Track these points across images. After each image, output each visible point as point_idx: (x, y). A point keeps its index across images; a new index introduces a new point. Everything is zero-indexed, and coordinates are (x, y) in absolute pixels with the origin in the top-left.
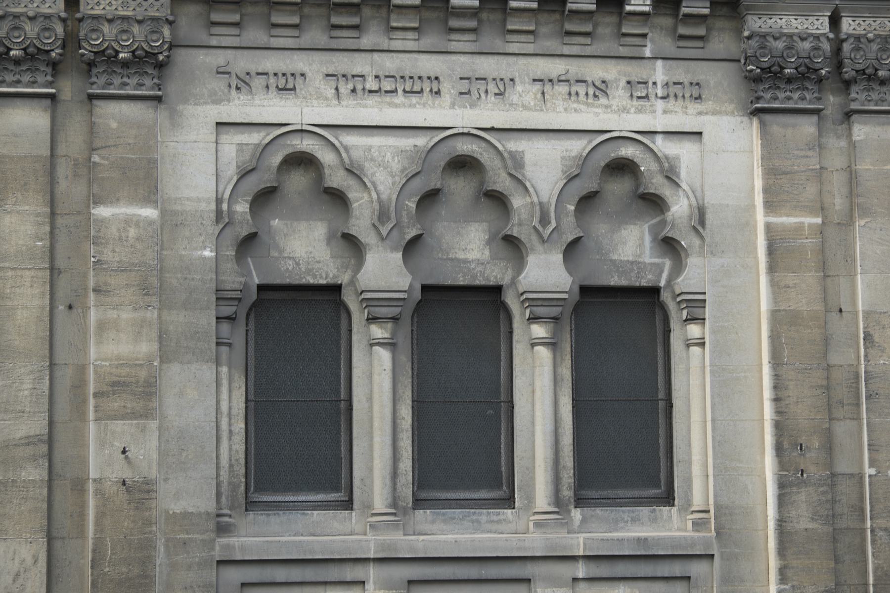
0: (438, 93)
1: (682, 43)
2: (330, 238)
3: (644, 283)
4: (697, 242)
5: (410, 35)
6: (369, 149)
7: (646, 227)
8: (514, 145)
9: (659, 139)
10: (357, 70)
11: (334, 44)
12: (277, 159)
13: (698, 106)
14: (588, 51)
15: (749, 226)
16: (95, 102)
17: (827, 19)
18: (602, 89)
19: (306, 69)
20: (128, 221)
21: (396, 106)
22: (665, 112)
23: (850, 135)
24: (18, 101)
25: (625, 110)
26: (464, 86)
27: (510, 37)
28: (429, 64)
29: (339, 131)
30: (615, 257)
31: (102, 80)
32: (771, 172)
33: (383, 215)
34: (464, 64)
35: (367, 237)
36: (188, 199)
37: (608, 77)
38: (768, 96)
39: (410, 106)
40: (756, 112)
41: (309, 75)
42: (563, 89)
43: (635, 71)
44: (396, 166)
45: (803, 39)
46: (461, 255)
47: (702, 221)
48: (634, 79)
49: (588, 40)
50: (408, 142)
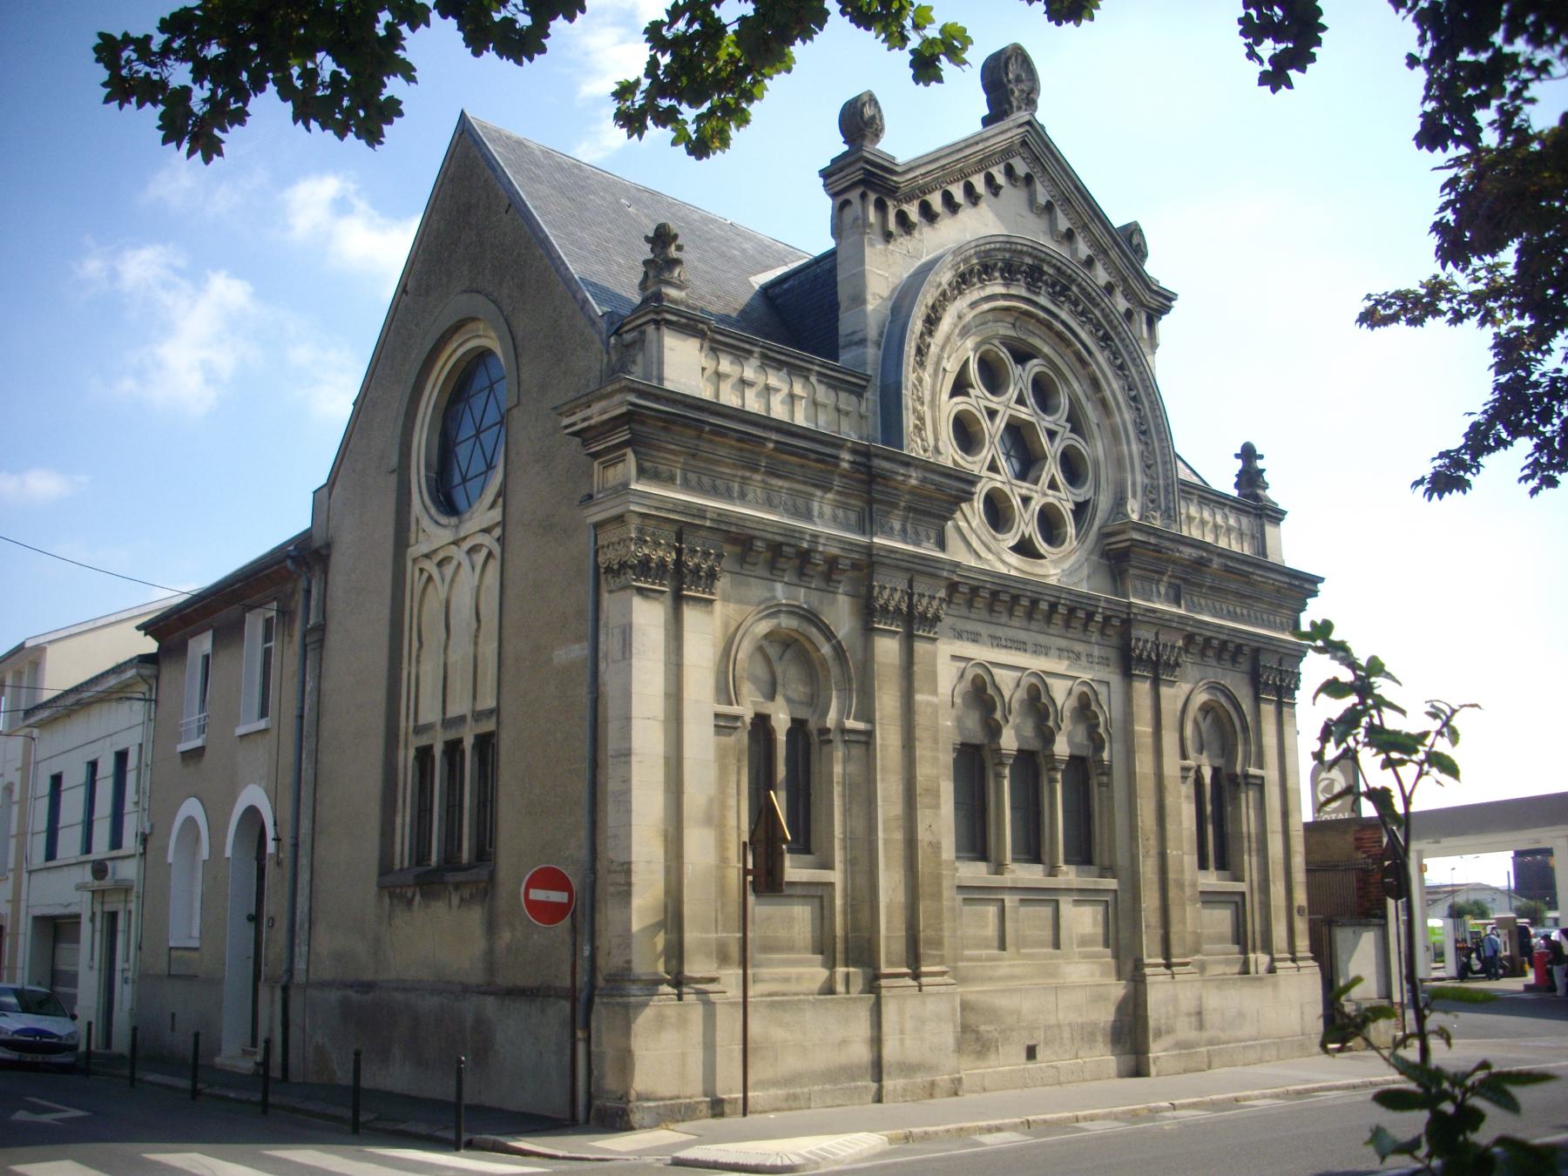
13: (1107, 669)
28: (1022, 635)
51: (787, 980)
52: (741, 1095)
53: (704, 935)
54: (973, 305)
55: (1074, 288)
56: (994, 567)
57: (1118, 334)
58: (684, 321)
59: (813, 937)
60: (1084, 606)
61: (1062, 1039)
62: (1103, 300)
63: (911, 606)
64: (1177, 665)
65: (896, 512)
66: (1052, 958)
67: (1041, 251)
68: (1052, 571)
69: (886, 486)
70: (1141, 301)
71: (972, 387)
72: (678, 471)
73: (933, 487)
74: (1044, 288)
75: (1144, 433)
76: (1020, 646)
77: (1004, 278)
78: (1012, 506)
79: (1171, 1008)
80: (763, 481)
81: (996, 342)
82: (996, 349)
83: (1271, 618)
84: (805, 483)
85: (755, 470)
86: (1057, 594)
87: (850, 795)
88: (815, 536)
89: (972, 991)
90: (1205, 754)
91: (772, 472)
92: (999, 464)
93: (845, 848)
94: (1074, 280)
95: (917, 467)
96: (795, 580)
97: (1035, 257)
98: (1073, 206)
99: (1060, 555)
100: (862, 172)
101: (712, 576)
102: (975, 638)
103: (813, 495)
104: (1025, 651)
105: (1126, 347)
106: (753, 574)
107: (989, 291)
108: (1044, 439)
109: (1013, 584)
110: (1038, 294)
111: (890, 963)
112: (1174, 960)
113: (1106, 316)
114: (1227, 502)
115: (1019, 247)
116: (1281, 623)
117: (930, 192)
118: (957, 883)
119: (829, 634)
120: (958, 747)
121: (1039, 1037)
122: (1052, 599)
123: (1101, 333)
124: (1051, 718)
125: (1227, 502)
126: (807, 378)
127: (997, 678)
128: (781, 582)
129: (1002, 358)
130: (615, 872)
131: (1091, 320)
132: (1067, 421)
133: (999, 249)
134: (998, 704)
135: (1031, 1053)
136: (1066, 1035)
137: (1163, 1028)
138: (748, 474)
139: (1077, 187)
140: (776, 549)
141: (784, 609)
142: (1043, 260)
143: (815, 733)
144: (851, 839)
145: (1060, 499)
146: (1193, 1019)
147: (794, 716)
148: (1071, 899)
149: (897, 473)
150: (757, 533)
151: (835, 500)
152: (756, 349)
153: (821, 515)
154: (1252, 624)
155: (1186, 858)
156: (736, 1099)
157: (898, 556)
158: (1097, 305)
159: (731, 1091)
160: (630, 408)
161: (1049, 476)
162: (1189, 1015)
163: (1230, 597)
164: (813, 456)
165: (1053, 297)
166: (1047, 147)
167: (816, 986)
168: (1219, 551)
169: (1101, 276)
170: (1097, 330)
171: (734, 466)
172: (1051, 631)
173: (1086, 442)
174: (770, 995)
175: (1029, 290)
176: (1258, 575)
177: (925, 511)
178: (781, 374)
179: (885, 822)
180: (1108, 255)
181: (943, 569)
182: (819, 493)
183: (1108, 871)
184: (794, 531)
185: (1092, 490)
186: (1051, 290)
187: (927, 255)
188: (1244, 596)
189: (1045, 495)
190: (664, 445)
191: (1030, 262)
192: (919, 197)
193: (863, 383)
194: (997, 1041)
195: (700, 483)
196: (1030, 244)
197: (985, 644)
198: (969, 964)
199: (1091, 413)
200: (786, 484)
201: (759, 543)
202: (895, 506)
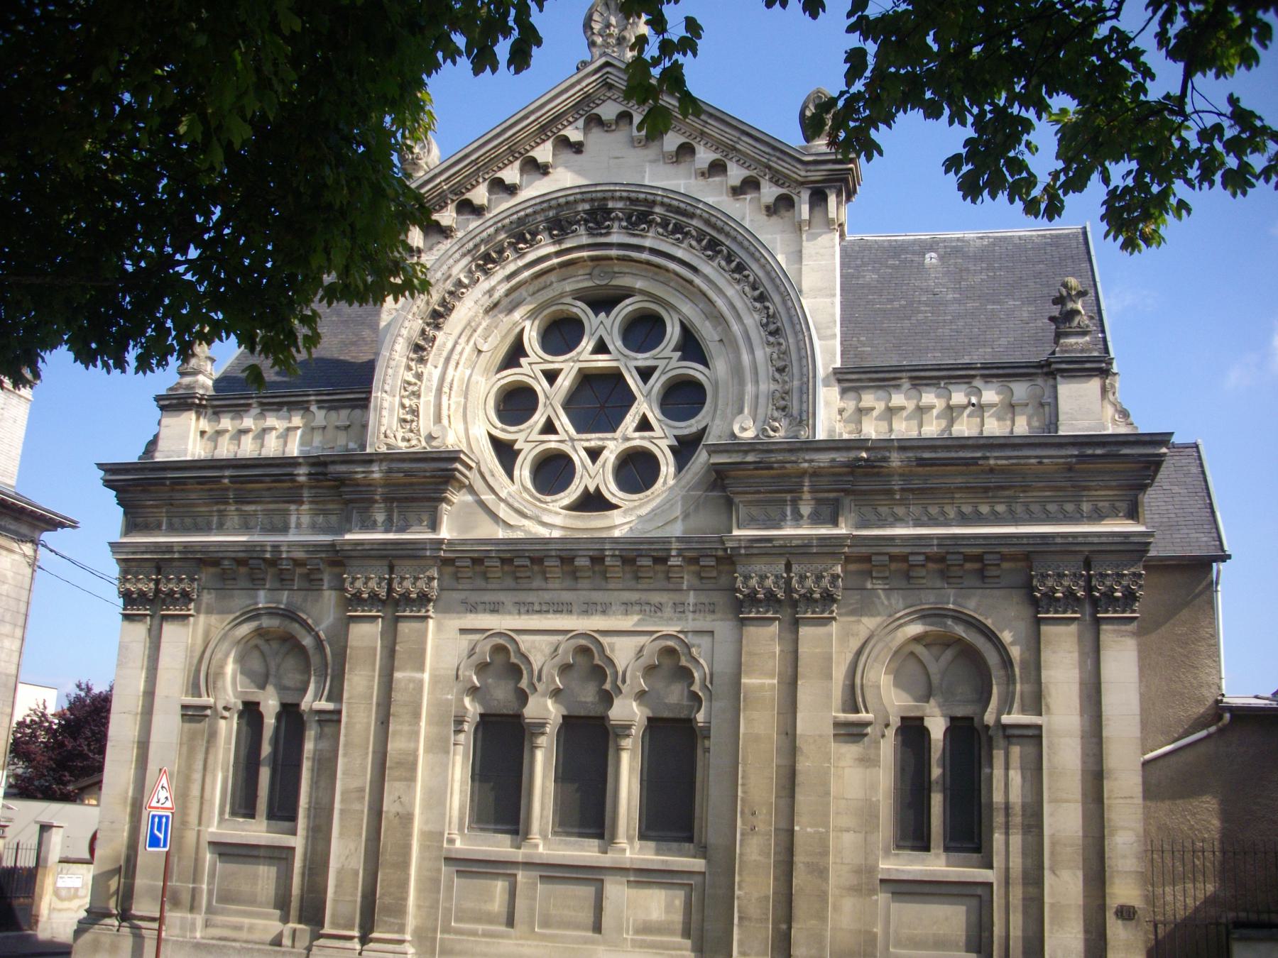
3: (682, 716)
5: (557, 581)
6: (533, 642)
7: (685, 684)
9: (690, 635)
10: (530, 600)
13: (713, 617)
14: (652, 586)
17: (783, 567)
18: (659, 608)
22: (694, 620)
25: (671, 619)
28: (567, 596)
30: (667, 701)
34: (584, 595)
37: (663, 601)
42: (637, 608)
43: (677, 597)
48: (677, 602)
49: (652, 581)
51: (238, 928)
55: (657, 210)
56: (530, 532)
57: (727, 235)
58: (175, 401)
59: (276, 894)
63: (390, 589)
65: (377, 505)
66: (585, 943)
73: (402, 475)
75: (775, 333)
77: (552, 236)
80: (237, 510)
81: (569, 300)
82: (565, 307)
85: (227, 503)
87: (318, 769)
88: (276, 547)
90: (932, 701)
91: (240, 501)
93: (309, 817)
95: (381, 461)
96: (277, 585)
97: (592, 200)
99: (636, 504)
102: (495, 609)
104: (570, 612)
105: (740, 244)
110: (608, 234)
111: (335, 925)
113: (707, 222)
117: (468, 190)
118: (444, 854)
119: (309, 629)
124: (609, 680)
126: (307, 409)
127: (523, 648)
134: (525, 672)
138: (222, 507)
142: (605, 199)
144: (315, 809)
147: (284, 701)
148: (625, 879)
149: (356, 472)
150: (221, 555)
151: (310, 509)
152: (250, 401)
153: (298, 526)
157: (367, 547)
158: (692, 216)
163: (957, 496)
164: (268, 479)
167: (269, 937)
168: (896, 444)
171: (206, 504)
172: (611, 586)
174: (220, 939)
175: (591, 234)
176: (997, 458)
177: (406, 498)
178: (281, 413)
179: (343, 793)
182: (293, 507)
183: (703, 851)
184: (255, 546)
185: (711, 415)
190: (143, 503)
191: (587, 207)
193: (363, 396)
196: (577, 191)
197: (510, 613)
199: (707, 332)
200: (259, 508)
202: (376, 502)
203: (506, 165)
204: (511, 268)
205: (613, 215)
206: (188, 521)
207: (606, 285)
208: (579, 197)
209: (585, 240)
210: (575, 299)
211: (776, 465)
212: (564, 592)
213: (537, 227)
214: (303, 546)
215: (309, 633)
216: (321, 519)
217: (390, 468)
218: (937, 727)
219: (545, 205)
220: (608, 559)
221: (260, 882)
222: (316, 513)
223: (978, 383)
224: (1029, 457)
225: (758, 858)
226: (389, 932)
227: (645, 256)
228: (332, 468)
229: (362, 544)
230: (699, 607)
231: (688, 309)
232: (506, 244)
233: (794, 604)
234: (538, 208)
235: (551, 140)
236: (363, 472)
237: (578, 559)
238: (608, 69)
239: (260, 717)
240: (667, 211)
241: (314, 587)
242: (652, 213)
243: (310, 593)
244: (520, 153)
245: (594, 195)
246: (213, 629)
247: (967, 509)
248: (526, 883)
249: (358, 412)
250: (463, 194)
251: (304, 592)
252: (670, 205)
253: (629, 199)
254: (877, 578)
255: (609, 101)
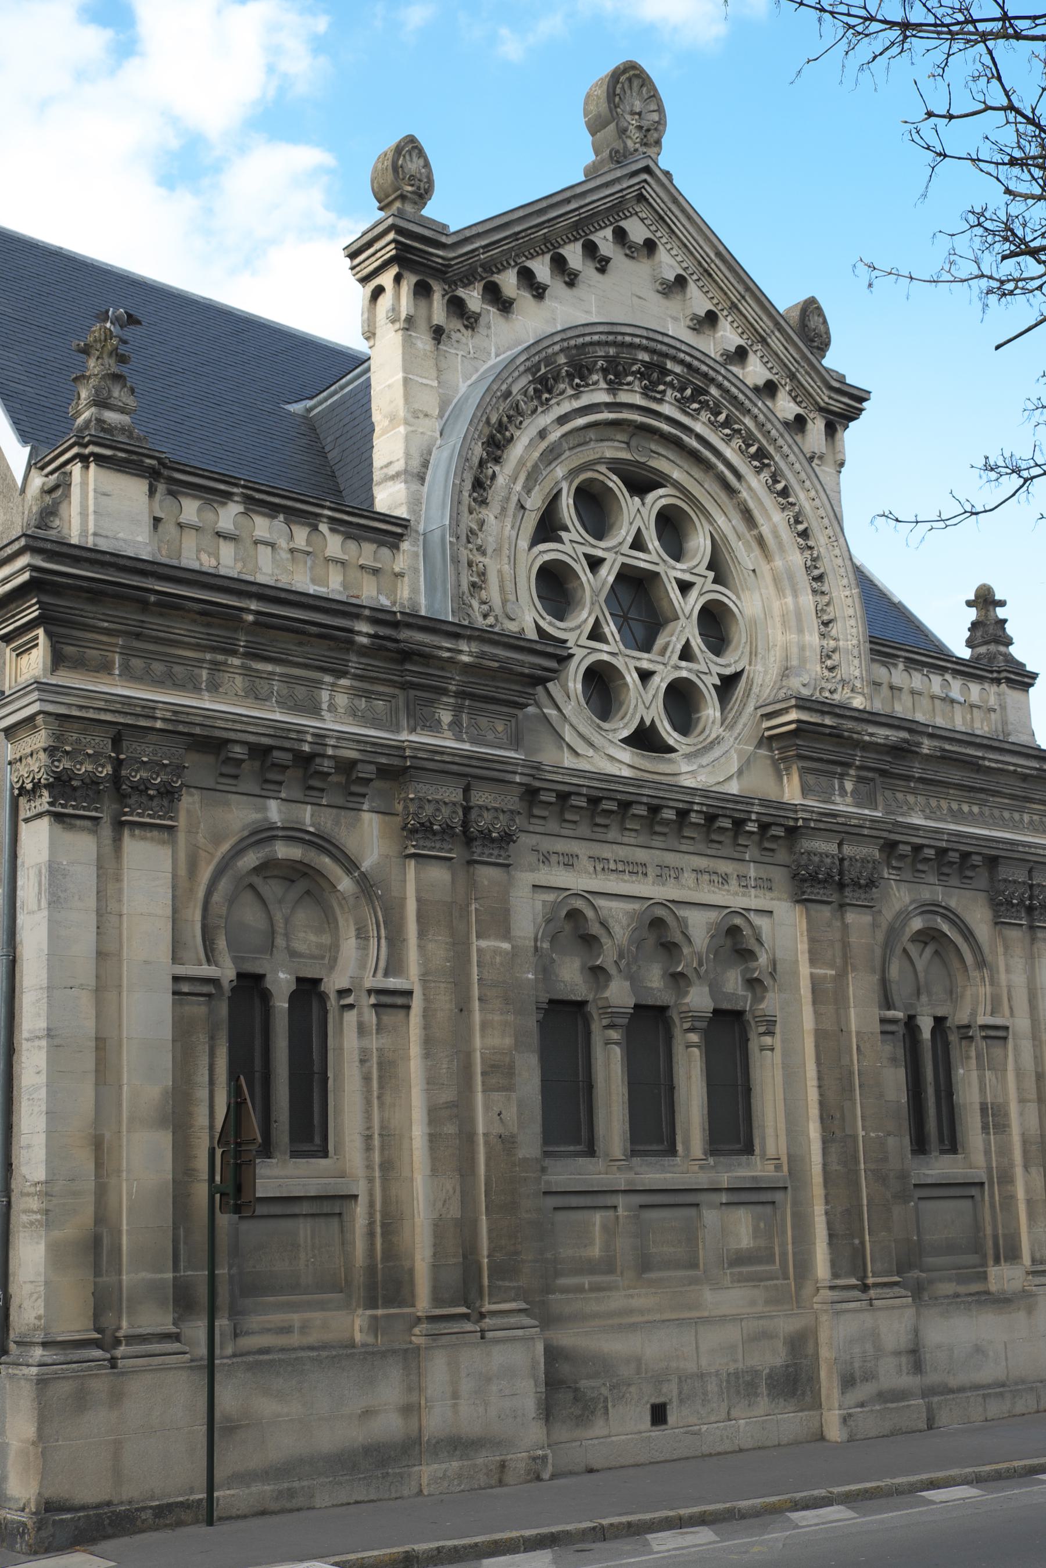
0: (646, 874)
1: (764, 853)
2: (583, 967)
4: (771, 982)
5: (633, 834)
8: (682, 912)
9: (752, 913)
10: (605, 855)
11: (594, 836)
12: (564, 913)
15: (796, 973)
16: (476, 866)
18: (725, 879)
19: (579, 852)
20: (496, 951)
21: (625, 881)
22: (756, 897)
23: (843, 918)
24: (433, 861)
25: (736, 894)
26: (658, 871)
27: (655, 837)
28: (641, 855)
29: (595, 896)
31: (479, 850)
32: (813, 941)
33: (621, 956)
35: (613, 970)
36: (519, 937)
38: (809, 890)
39: (633, 882)
40: (798, 902)
41: (580, 856)
42: (706, 877)
44: (624, 922)
45: (827, 856)
46: (649, 985)
47: (775, 969)
50: (636, 906)
52: (203, 1496)
53: (159, 1276)
54: (562, 420)
55: (714, 391)
60: (728, 813)
61: (705, 1394)
62: (756, 405)
63: (465, 824)
64: (871, 883)
65: (445, 699)
67: (662, 343)
68: (685, 768)
69: (427, 666)
70: (817, 403)
71: (566, 529)
72: (117, 657)
73: (496, 665)
74: (669, 392)
76: (638, 869)
77: (610, 383)
78: (626, 684)
79: (869, 1346)
80: (243, 667)
81: (603, 468)
82: (601, 478)
83: (1016, 816)
84: (306, 666)
85: (233, 653)
86: (688, 798)
88: (320, 737)
89: (567, 1338)
92: (606, 630)
94: (712, 380)
95: (470, 638)
96: (298, 795)
97: (653, 352)
98: (715, 281)
100: (393, 246)
101: (169, 794)
102: (569, 862)
103: (322, 682)
106: (233, 789)
107: (585, 400)
108: (674, 593)
109: (621, 788)
110: (660, 401)
112: (870, 1281)
113: (761, 426)
114: (949, 665)
115: (628, 339)
116: (1031, 822)
117: (499, 271)
119: (350, 864)
120: (545, 1006)
121: (670, 1392)
122: (681, 805)
123: (753, 450)
125: (949, 665)
126: (315, 528)
128: (277, 798)
129: (611, 489)
130: (28, 1194)
131: (739, 431)
132: (710, 567)
133: (599, 343)
135: (659, 1415)
136: (712, 1387)
137: (858, 1374)
138: (220, 658)
139: (719, 254)
140: (260, 752)
141: (280, 833)
142: (666, 356)
143: (333, 996)
145: (698, 673)
146: (904, 1359)
149: (440, 648)
150: (232, 736)
151: (352, 687)
152: (235, 490)
153: (332, 708)
154: (986, 825)
155: (891, 1141)
156: (201, 1500)
159: (192, 1491)
160: (35, 574)
161: (683, 642)
162: (898, 1353)
163: (951, 791)
165: (682, 404)
166: (675, 201)
169: (755, 371)
170: (748, 446)
171: (197, 647)
173: (739, 597)
175: (645, 395)
176: (990, 760)
180: (768, 345)
181: (515, 773)
182: (328, 679)
184: (289, 730)
186: (679, 396)
187: (497, 355)
188: (972, 789)
189: (677, 668)
191: (645, 357)
192: (483, 279)
193: (399, 530)
194: (606, 1400)
195: (148, 670)
196: (644, 333)
198: (563, 1296)
200: (278, 669)
201: (238, 749)
202: (444, 692)
203: (538, 254)
204: (566, 407)
205: (669, 379)
206: (158, 667)
207: (643, 463)
208: (644, 342)
209: (638, 400)
210: (609, 469)
211: (846, 734)
212: (638, 849)
213: (596, 362)
214: (358, 742)
215: (348, 872)
216: (363, 703)
217: (483, 653)
218: (926, 1025)
219: (611, 338)
220: (693, 815)
221: (302, 1255)
222: (357, 693)
223: (948, 677)
224: (1009, 763)
225: (838, 1168)
226: (505, 1301)
227: (694, 443)
228: (405, 634)
229: (442, 753)
230: (760, 882)
231: (728, 523)
232: (563, 373)
233: (841, 886)
234: (603, 338)
235: (581, 242)
236: (449, 650)
237: (665, 810)
238: (645, 176)
239: (266, 996)
240: (721, 396)
241: (351, 805)
242: (707, 393)
243: (343, 813)
244: (552, 245)
245: (659, 346)
246: (203, 854)
247: (955, 806)
248: (627, 1217)
249: (385, 551)
250: (493, 273)
251: (334, 811)
252: (728, 391)
253: (689, 366)
254: (894, 868)
255: (635, 218)
